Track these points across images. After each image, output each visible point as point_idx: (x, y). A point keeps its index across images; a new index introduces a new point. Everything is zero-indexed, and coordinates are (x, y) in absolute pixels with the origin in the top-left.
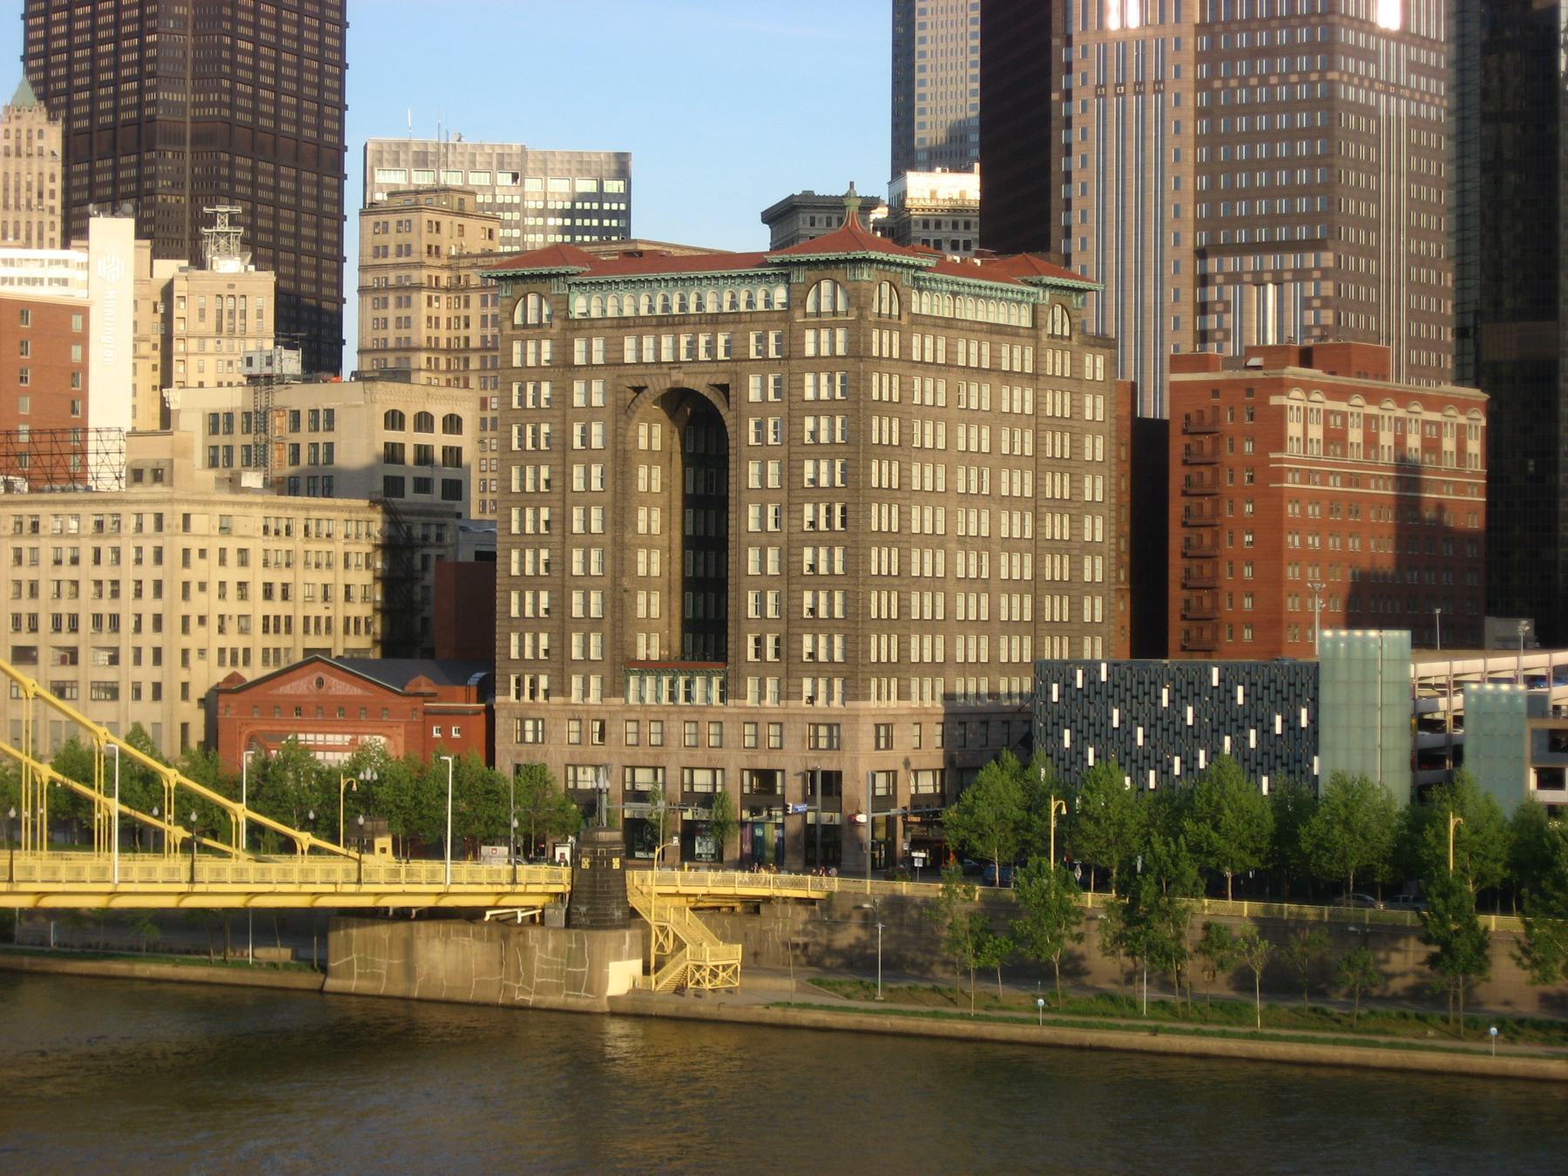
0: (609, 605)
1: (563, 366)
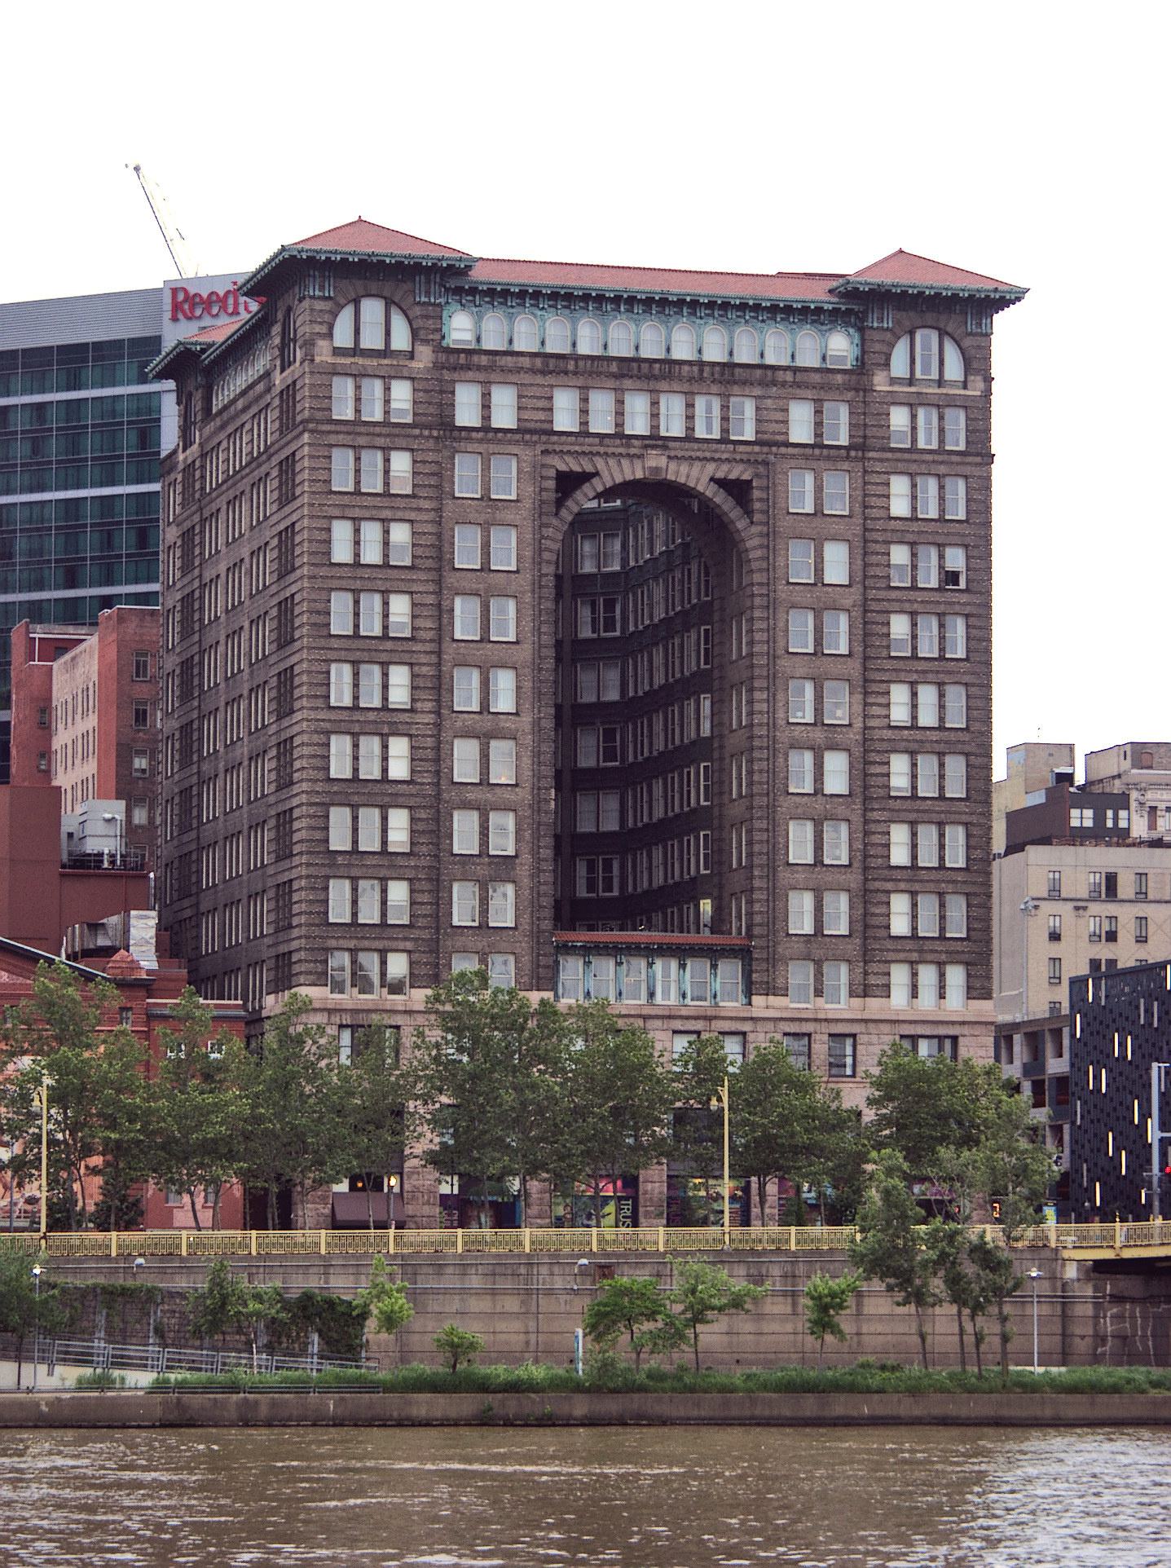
0: (527, 835)
1: (436, 430)
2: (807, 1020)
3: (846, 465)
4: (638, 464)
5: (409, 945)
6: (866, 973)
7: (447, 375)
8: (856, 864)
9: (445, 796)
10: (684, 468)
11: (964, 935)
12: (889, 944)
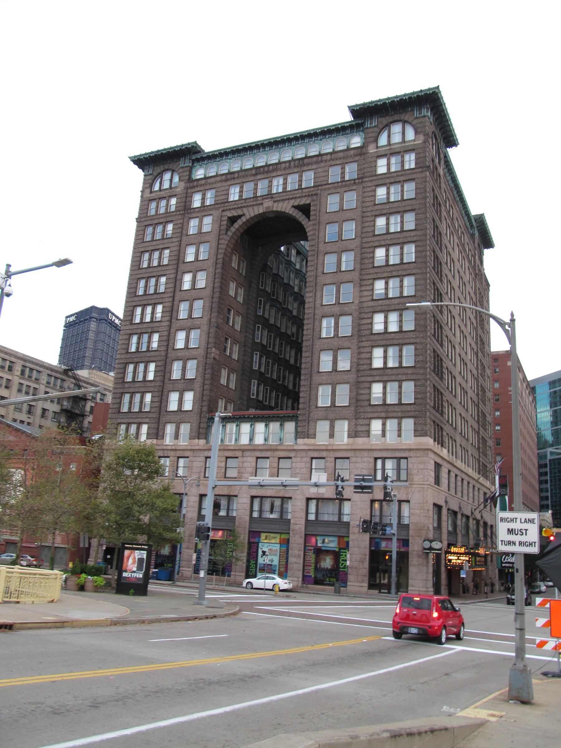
2: (322, 450)
3: (354, 187)
4: (261, 207)
5: (147, 420)
6: (356, 425)
7: (189, 191)
8: (353, 370)
9: (169, 355)
10: (280, 204)
11: (413, 402)
12: (369, 409)
